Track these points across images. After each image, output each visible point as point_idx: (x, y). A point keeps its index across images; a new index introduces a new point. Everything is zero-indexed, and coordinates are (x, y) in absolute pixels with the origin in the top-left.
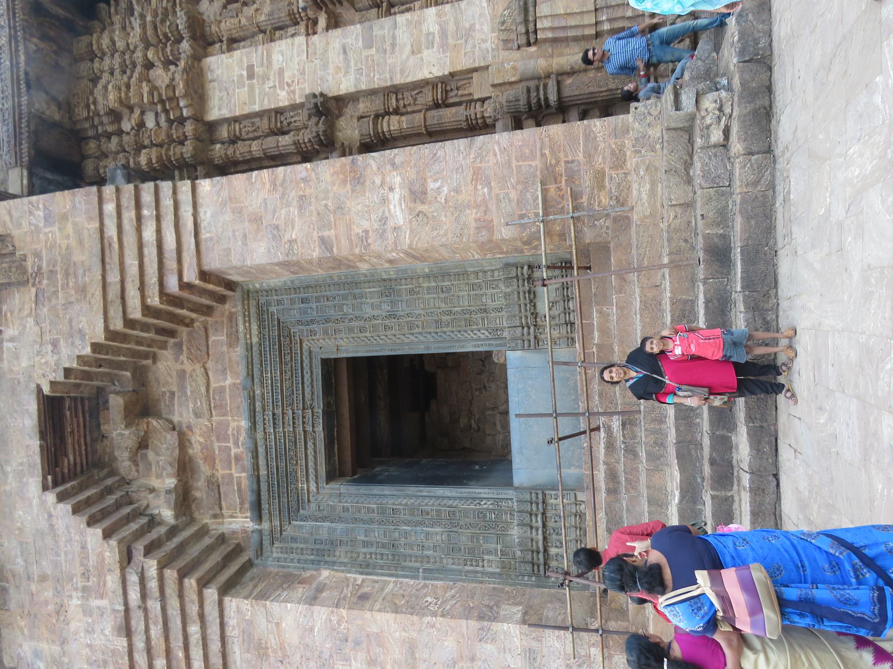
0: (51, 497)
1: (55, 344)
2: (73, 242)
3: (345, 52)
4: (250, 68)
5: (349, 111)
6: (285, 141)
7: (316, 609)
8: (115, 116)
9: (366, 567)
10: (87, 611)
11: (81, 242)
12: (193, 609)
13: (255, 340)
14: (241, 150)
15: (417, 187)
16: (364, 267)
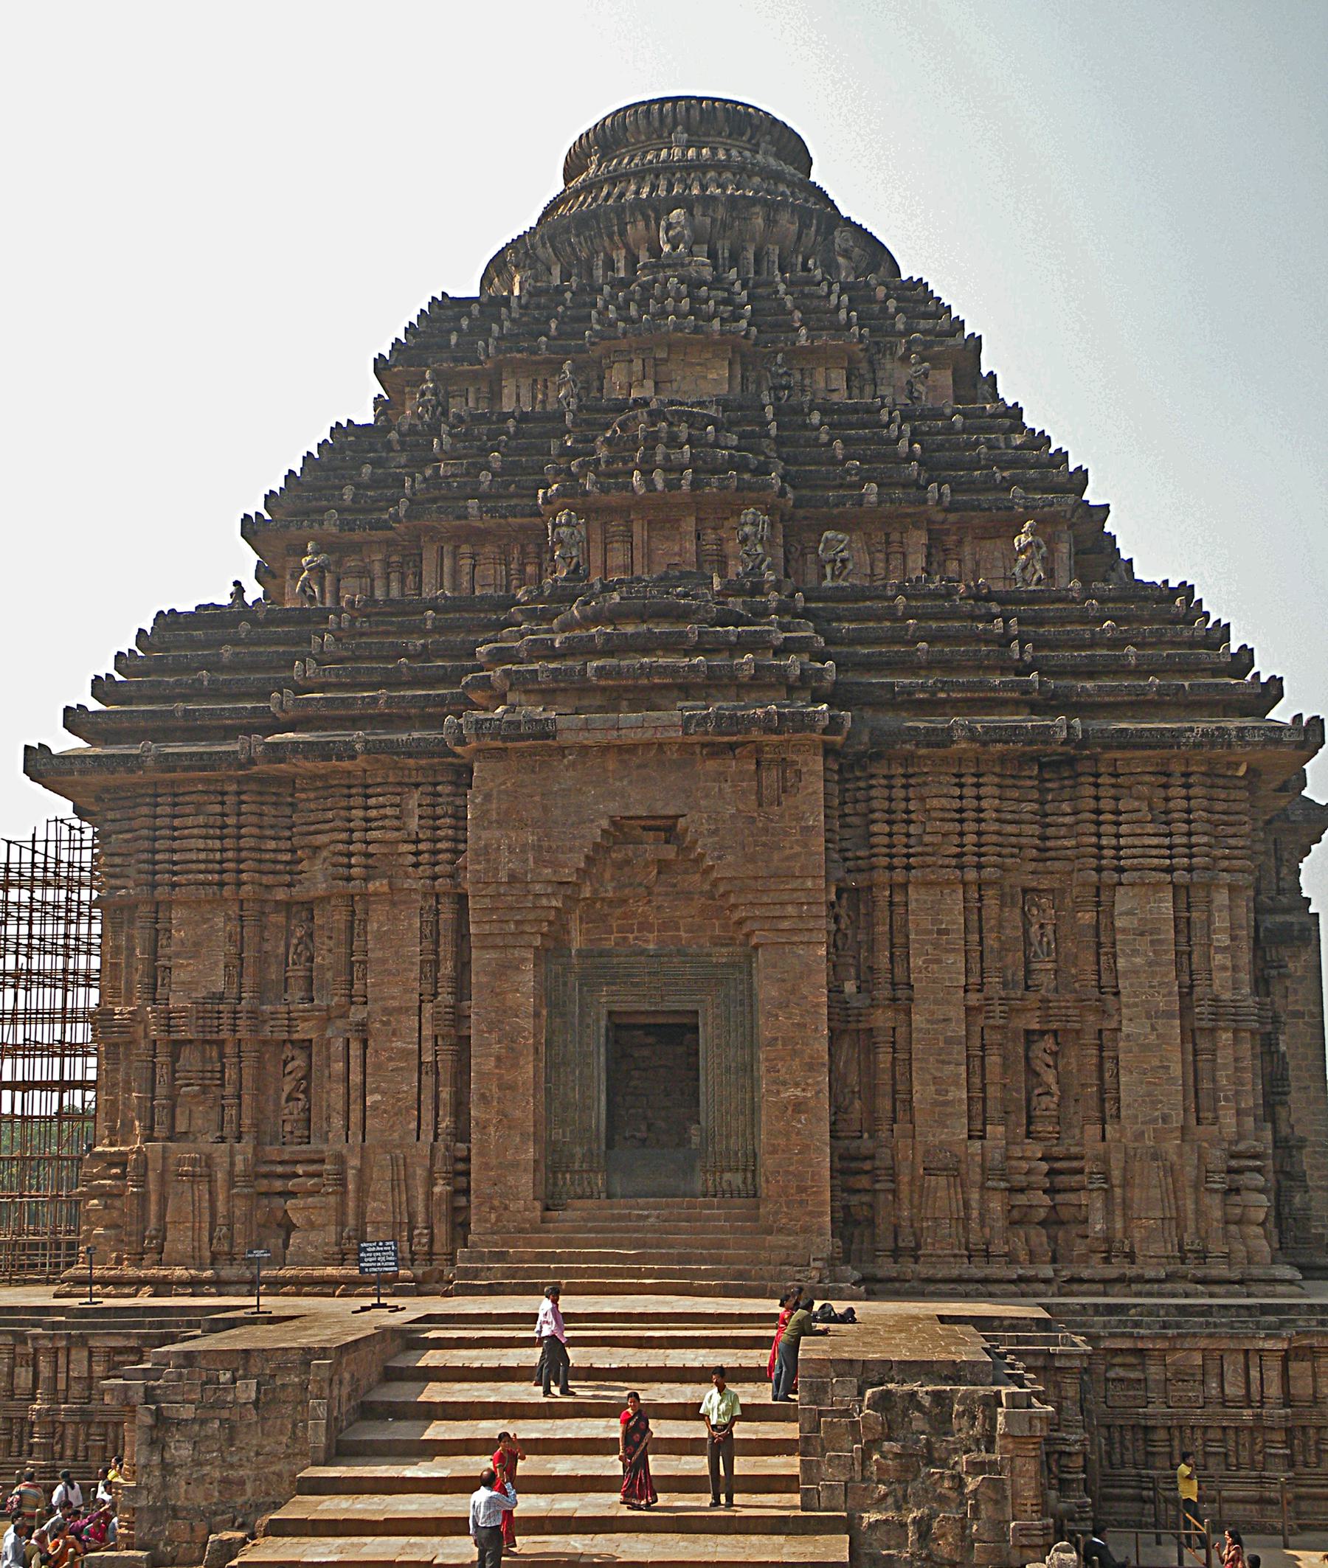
0: (605, 823)
1: (714, 832)
2: (787, 852)
3: (944, 1020)
4: (946, 932)
5: (902, 1016)
6: (883, 959)
7: (531, 1020)
8: (922, 799)
9: (549, 1043)
10: (524, 847)
11: (788, 858)
12: (528, 928)
13: (714, 960)
14: (882, 914)
15: (803, 1107)
16: (762, 1056)
